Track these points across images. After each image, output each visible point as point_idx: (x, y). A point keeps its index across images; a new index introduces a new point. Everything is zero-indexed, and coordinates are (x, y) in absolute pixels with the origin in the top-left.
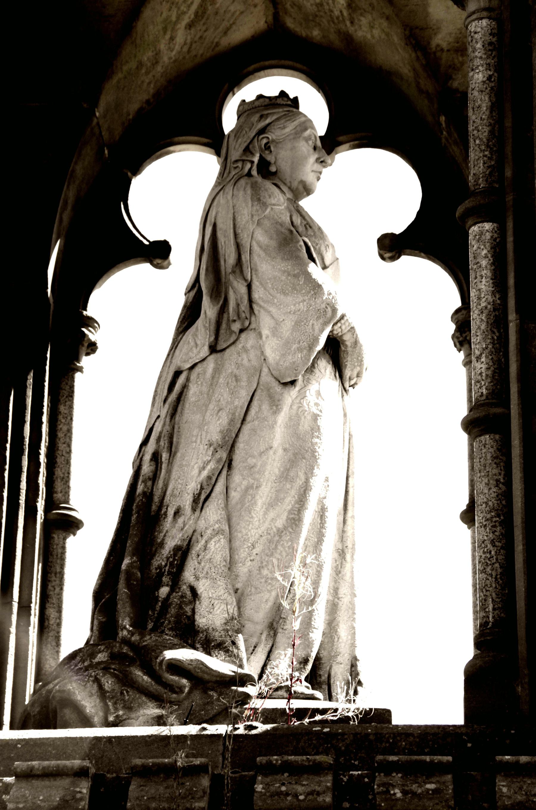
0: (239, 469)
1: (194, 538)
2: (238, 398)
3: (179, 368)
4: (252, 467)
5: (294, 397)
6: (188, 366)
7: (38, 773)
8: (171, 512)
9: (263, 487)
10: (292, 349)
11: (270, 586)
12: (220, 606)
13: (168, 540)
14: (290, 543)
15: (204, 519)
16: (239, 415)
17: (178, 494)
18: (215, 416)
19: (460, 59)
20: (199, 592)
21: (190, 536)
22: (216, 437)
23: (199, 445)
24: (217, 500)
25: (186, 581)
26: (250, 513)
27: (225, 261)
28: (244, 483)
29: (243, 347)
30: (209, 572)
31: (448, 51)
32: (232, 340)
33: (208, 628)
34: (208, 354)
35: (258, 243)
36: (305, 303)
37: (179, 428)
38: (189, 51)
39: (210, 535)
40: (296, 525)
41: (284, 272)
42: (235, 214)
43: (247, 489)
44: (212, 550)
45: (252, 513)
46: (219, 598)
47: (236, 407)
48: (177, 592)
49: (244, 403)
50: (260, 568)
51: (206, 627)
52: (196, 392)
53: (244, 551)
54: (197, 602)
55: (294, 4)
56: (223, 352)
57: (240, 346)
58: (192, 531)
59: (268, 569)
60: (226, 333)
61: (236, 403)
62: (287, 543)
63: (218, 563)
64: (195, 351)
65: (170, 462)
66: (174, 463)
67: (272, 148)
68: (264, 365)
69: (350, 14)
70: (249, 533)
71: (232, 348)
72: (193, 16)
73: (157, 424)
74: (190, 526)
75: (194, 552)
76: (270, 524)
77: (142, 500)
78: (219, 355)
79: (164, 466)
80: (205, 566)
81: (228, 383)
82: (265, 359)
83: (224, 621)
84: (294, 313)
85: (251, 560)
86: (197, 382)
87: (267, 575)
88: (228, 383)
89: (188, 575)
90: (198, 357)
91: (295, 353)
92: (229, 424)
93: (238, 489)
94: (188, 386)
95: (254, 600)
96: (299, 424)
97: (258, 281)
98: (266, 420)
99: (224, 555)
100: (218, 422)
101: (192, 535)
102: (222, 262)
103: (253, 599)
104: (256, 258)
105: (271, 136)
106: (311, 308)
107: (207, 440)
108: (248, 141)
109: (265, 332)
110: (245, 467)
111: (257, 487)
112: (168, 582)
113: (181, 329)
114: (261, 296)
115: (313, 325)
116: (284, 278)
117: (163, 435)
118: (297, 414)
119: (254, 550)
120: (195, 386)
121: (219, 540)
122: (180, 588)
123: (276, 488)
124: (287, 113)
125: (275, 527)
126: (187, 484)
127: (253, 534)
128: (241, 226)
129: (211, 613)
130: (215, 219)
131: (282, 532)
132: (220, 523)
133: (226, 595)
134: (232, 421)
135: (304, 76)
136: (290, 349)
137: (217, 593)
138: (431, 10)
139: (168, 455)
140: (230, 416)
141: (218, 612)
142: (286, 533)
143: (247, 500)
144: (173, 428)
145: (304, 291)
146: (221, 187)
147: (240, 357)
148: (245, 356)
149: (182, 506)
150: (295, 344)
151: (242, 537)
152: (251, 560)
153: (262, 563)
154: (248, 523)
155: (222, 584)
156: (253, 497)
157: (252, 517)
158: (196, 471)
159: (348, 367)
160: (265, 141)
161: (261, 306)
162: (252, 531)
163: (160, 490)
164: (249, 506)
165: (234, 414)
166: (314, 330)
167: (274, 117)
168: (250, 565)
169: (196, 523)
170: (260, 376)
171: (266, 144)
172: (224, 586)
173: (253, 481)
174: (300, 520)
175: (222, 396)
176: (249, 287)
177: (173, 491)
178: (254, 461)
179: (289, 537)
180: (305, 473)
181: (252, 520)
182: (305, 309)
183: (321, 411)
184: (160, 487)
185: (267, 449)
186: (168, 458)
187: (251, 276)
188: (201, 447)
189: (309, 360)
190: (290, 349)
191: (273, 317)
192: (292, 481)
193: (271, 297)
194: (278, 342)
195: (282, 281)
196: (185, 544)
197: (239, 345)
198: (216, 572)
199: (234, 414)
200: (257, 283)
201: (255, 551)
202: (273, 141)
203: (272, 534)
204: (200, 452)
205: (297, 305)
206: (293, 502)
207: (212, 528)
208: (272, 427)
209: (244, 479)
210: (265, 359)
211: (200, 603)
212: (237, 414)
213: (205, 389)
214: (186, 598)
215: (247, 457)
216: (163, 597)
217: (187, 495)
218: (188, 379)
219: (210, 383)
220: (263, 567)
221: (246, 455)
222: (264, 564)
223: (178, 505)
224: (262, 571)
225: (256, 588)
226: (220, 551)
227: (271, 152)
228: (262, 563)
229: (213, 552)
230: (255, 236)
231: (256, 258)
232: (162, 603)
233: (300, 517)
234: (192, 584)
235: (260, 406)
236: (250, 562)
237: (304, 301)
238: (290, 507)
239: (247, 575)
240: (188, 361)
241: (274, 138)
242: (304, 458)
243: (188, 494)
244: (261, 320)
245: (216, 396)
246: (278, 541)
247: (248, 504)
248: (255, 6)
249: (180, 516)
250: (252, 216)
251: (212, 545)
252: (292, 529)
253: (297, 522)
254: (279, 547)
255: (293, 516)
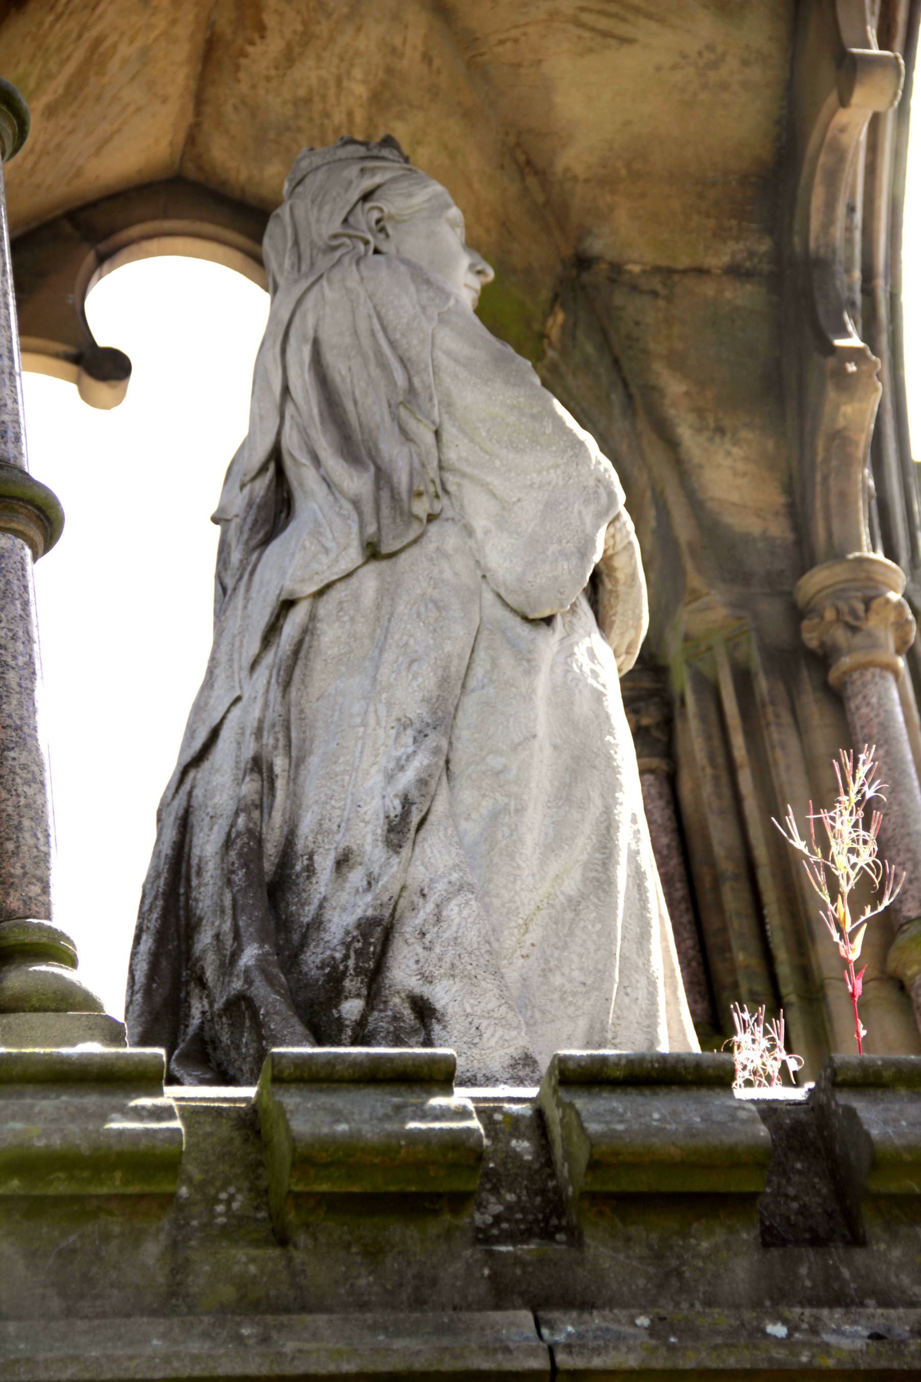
0: (469, 777)
1: (403, 903)
2: (449, 639)
3: (292, 592)
4: (501, 772)
5: (555, 649)
6: (314, 588)
7: (618, 1073)
8: (325, 864)
9: (530, 810)
10: (549, 552)
11: (572, 1008)
12: (495, 1031)
13: (333, 915)
14: (598, 926)
15: (422, 863)
16: (457, 671)
17: (335, 827)
18: (404, 673)
19: (608, 198)
20: (438, 1006)
21: (395, 897)
22: (416, 710)
23: (375, 730)
24: (442, 828)
25: (399, 987)
26: (513, 859)
27: (355, 402)
28: (484, 803)
29: (438, 549)
30: (458, 964)
31: (587, 181)
32: (412, 535)
33: (475, 1076)
34: (360, 561)
35: (448, 354)
36: (559, 472)
37: (302, 711)
38: (33, 171)
39: (444, 894)
40: (604, 891)
41: (513, 407)
42: (379, 308)
43: (495, 817)
44: (456, 921)
45: (518, 860)
46: (488, 1015)
47: (449, 656)
48: (381, 1011)
49: (463, 649)
50: (545, 973)
51: (468, 1074)
52: (339, 638)
53: (512, 934)
54: (437, 1027)
55: (244, 103)
56: (394, 560)
57: (432, 547)
58: (398, 887)
59: (563, 974)
60: (394, 523)
61: (448, 648)
62: (593, 926)
63: (475, 946)
64: (325, 560)
65: (294, 778)
66: (301, 778)
67: (390, 231)
68: (484, 586)
69: (370, 119)
70: (517, 898)
71: (415, 551)
72: (61, 91)
73: (231, 716)
74: (393, 877)
75: (408, 929)
76: (553, 887)
77: (248, 843)
78: (384, 565)
79: (280, 784)
80: (443, 954)
81: (419, 614)
82: (484, 577)
83: (507, 1061)
84: (540, 487)
85: (523, 956)
86: (338, 618)
87: (563, 985)
88: (419, 614)
89: (403, 974)
90: (336, 570)
91: (556, 560)
92: (440, 687)
93: (474, 816)
94: (315, 628)
95: (542, 1035)
96: (572, 703)
97: (454, 426)
98: (512, 685)
99: (483, 931)
100: (415, 684)
101: (400, 896)
102: (349, 406)
103: (540, 1032)
104: (447, 380)
105: (388, 208)
106: (571, 481)
107: (393, 718)
108: (348, 208)
109: (480, 523)
110: (484, 773)
111: (517, 811)
112: (359, 989)
113: (253, 543)
114: (464, 454)
115: (580, 512)
116: (512, 419)
117: (266, 725)
118: (565, 683)
119: (528, 936)
120: (336, 625)
121: (467, 903)
122: (385, 1002)
123: (552, 817)
124: (408, 173)
125: (563, 893)
126: (361, 804)
127: (526, 901)
128: (399, 327)
129: (475, 1045)
130: (316, 331)
131: (579, 903)
132: (461, 870)
133: (504, 1009)
134: (444, 681)
135: (238, 257)
136: (543, 552)
137: (483, 1004)
138: (558, 99)
139: (287, 761)
140: (440, 672)
141: (492, 1042)
142: (587, 907)
143: (500, 836)
144: (289, 711)
145: (554, 448)
146: (312, 279)
147: (433, 564)
148: (445, 565)
149: (355, 848)
150: (552, 544)
151: (503, 906)
152: (523, 956)
153: (547, 961)
154: (511, 878)
155: (490, 986)
156: (514, 829)
157: (519, 867)
158: (376, 779)
159: (615, 626)
160: (376, 215)
161: (464, 475)
162: (523, 894)
163: (277, 831)
164: (507, 846)
165: (446, 668)
166: (583, 523)
167: (388, 175)
168: (523, 967)
169: (406, 871)
170: (481, 607)
171: (378, 221)
172: (496, 991)
173: (506, 800)
174: (611, 883)
175: (411, 636)
176: (437, 434)
177: (321, 825)
178: (503, 760)
179: (594, 914)
180: (602, 795)
181: (519, 872)
182: (561, 483)
183: (604, 686)
184: (277, 825)
185: (526, 739)
186: (287, 767)
187: (440, 416)
188: (381, 733)
189: (583, 576)
190: (543, 552)
191: (494, 495)
192: (582, 807)
193: (488, 457)
194: (513, 541)
195: (508, 424)
196: (387, 913)
197: (430, 545)
198: (474, 963)
199: (446, 668)
200: (454, 431)
201: (531, 938)
202: (391, 218)
203: (558, 907)
204: (380, 742)
205: (545, 473)
206: (589, 848)
207: (445, 880)
208: (528, 698)
209: (484, 796)
210: (484, 577)
211: (445, 1027)
212: (453, 669)
213: (362, 628)
214: (404, 1021)
215: (484, 754)
216: (354, 1018)
217: (362, 825)
218: (313, 617)
219: (372, 616)
220: (551, 970)
221: (481, 750)
222: (553, 963)
223: (342, 846)
224: (551, 978)
225: (543, 1012)
226: (474, 923)
227: (387, 236)
228: (547, 961)
229: (459, 925)
230: (438, 341)
231: (448, 380)
232: (353, 1029)
233: (609, 878)
234: (417, 991)
235: (494, 662)
236: (521, 960)
237: (557, 466)
238: (584, 857)
239: (519, 985)
240: (311, 579)
241: (393, 211)
242: (594, 767)
243: (367, 823)
244: (466, 502)
245: (396, 637)
246: (573, 921)
247: (504, 842)
248: (165, 100)
249: (351, 868)
250: (424, 308)
251: (452, 910)
252: (599, 898)
253: (605, 886)
254: (578, 932)
255: (594, 874)
